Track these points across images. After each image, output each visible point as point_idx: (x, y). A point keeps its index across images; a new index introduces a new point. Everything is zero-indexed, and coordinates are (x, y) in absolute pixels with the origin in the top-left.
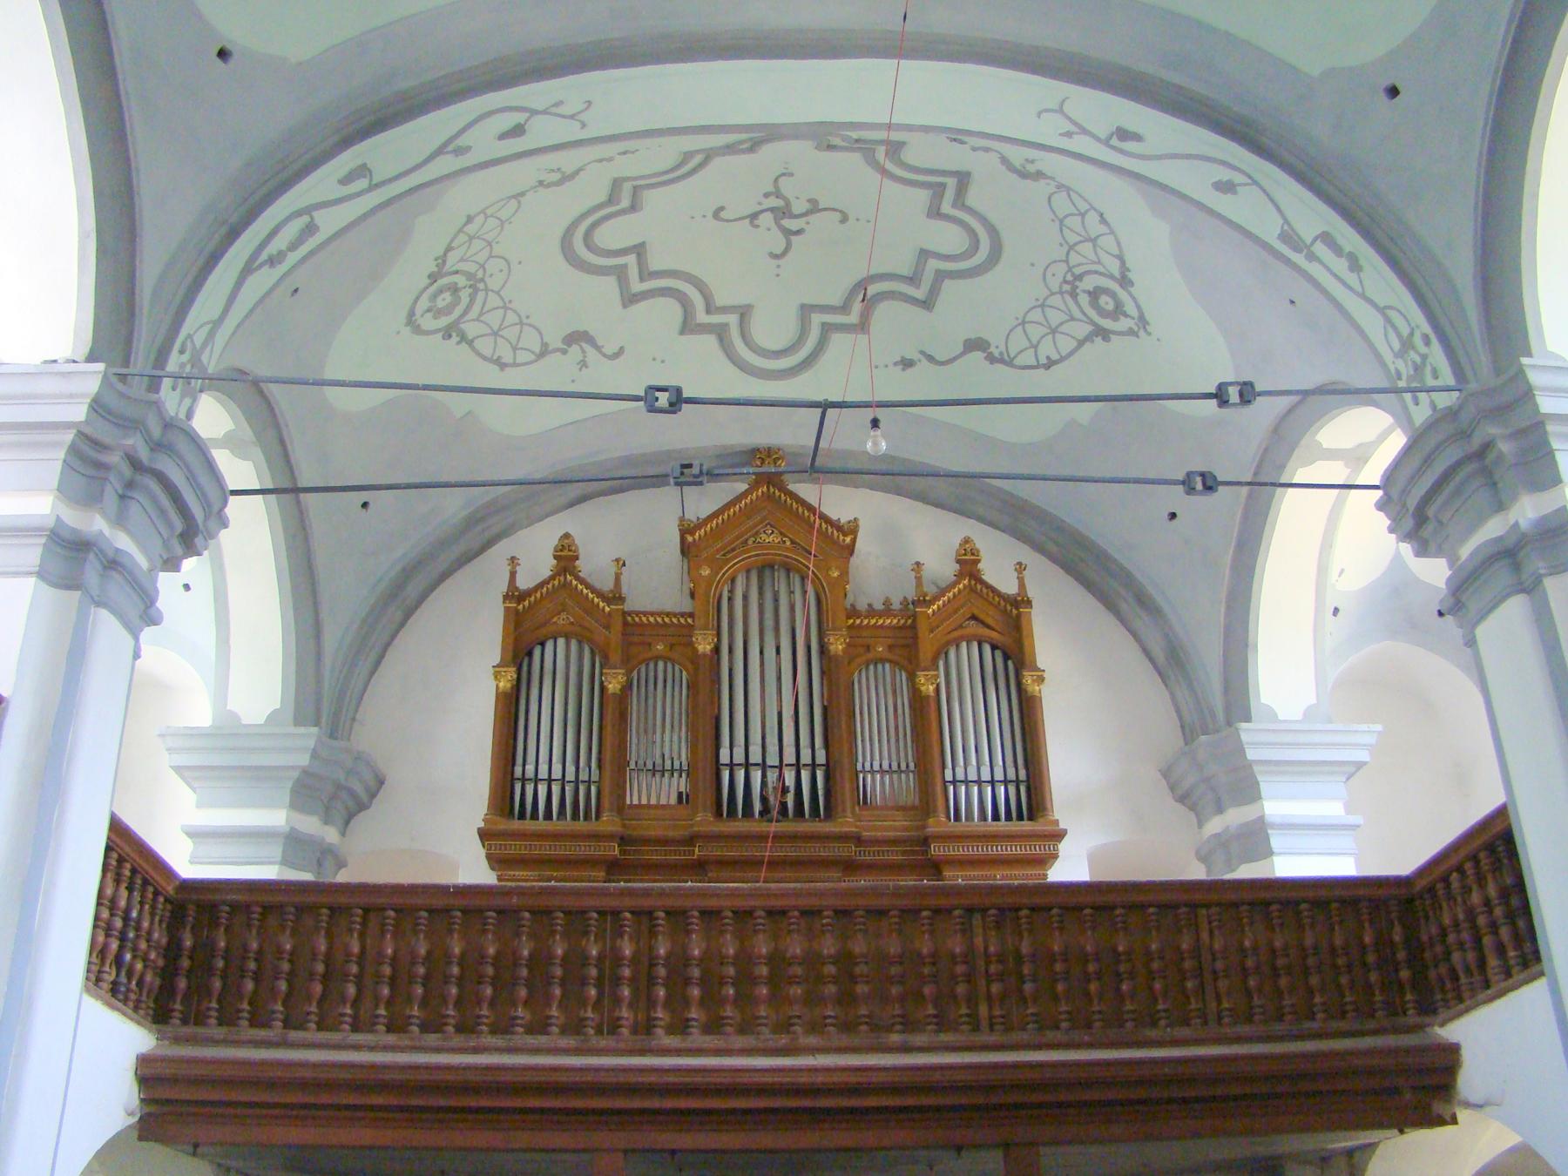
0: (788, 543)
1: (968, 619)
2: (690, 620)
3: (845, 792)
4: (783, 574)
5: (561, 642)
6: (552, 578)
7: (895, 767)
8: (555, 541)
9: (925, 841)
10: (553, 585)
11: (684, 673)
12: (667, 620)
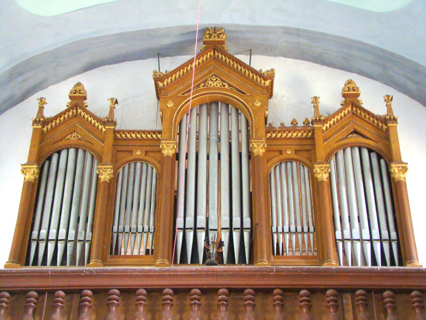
0: (227, 86)
1: (352, 133)
2: (159, 136)
4: (224, 106)
5: (72, 151)
6: (68, 110)
7: (299, 229)
10: (69, 115)
11: (154, 169)
12: (144, 136)
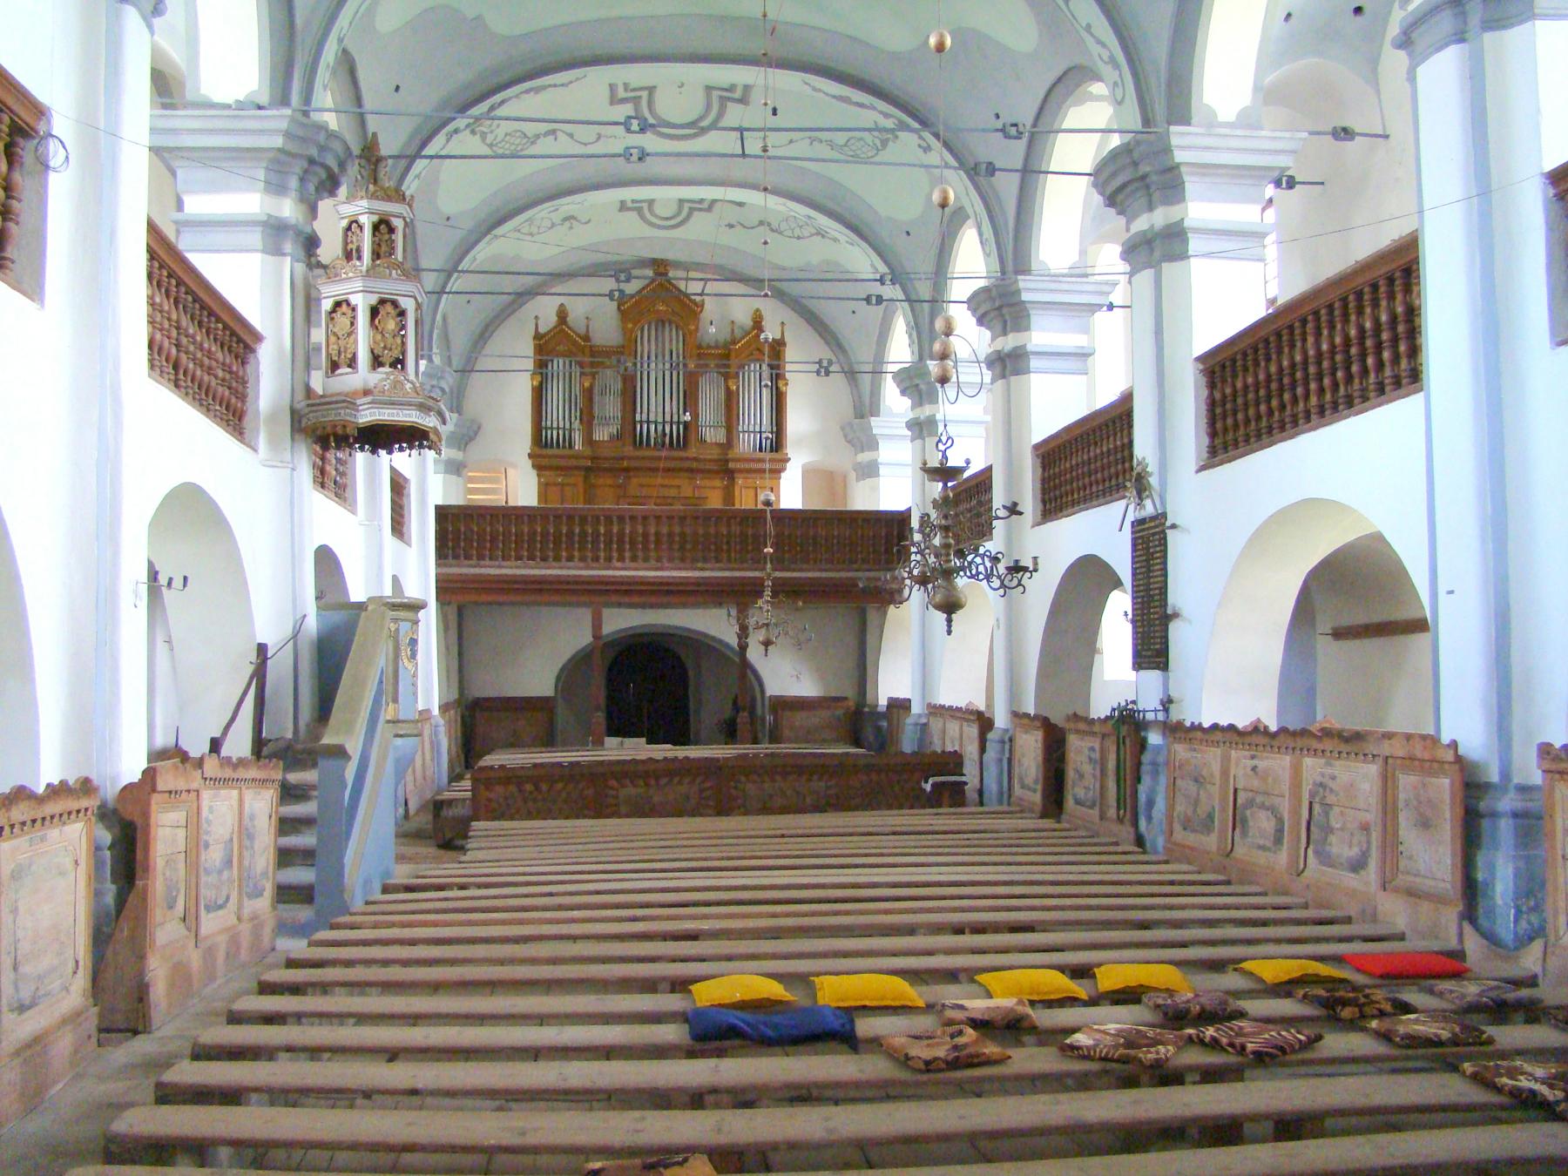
3: (692, 437)
6: (555, 327)
8: (556, 308)
9: (727, 461)
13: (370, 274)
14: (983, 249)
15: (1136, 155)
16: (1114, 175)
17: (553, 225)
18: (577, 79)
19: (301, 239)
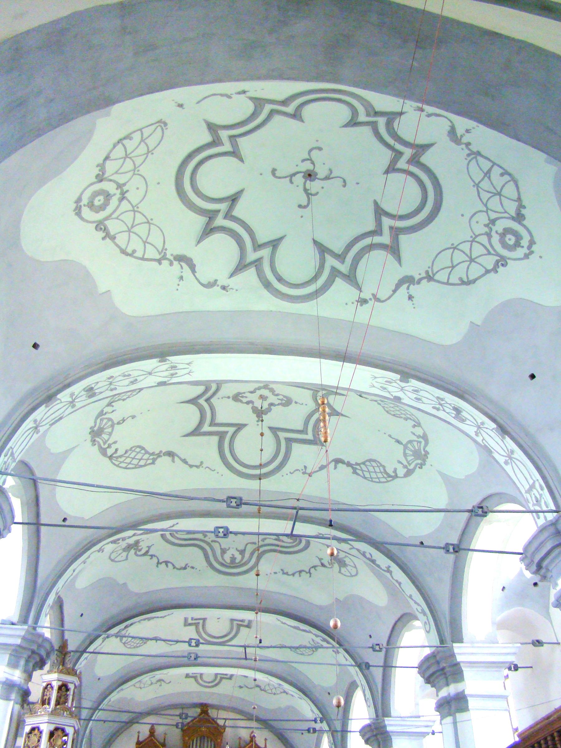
6: (148, 738)
13: (53, 713)
14: (367, 704)
15: (438, 658)
16: (428, 668)
17: (152, 683)
18: (169, 615)
19: (21, 692)
